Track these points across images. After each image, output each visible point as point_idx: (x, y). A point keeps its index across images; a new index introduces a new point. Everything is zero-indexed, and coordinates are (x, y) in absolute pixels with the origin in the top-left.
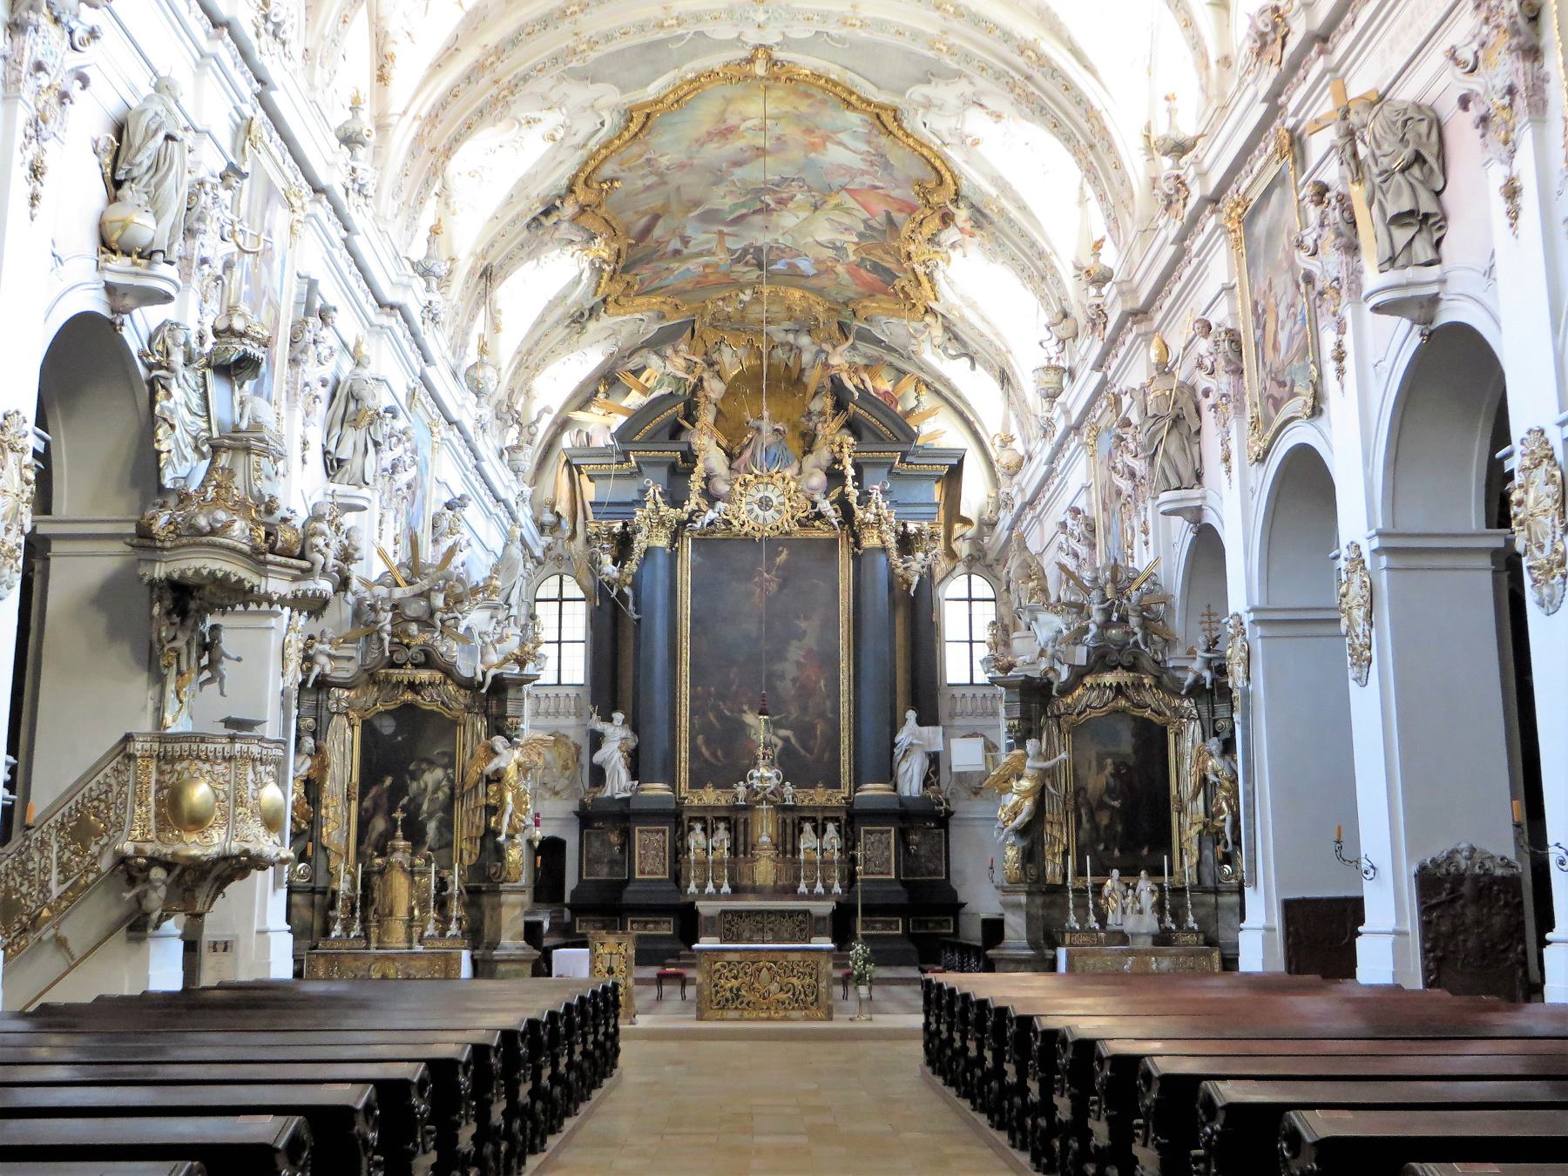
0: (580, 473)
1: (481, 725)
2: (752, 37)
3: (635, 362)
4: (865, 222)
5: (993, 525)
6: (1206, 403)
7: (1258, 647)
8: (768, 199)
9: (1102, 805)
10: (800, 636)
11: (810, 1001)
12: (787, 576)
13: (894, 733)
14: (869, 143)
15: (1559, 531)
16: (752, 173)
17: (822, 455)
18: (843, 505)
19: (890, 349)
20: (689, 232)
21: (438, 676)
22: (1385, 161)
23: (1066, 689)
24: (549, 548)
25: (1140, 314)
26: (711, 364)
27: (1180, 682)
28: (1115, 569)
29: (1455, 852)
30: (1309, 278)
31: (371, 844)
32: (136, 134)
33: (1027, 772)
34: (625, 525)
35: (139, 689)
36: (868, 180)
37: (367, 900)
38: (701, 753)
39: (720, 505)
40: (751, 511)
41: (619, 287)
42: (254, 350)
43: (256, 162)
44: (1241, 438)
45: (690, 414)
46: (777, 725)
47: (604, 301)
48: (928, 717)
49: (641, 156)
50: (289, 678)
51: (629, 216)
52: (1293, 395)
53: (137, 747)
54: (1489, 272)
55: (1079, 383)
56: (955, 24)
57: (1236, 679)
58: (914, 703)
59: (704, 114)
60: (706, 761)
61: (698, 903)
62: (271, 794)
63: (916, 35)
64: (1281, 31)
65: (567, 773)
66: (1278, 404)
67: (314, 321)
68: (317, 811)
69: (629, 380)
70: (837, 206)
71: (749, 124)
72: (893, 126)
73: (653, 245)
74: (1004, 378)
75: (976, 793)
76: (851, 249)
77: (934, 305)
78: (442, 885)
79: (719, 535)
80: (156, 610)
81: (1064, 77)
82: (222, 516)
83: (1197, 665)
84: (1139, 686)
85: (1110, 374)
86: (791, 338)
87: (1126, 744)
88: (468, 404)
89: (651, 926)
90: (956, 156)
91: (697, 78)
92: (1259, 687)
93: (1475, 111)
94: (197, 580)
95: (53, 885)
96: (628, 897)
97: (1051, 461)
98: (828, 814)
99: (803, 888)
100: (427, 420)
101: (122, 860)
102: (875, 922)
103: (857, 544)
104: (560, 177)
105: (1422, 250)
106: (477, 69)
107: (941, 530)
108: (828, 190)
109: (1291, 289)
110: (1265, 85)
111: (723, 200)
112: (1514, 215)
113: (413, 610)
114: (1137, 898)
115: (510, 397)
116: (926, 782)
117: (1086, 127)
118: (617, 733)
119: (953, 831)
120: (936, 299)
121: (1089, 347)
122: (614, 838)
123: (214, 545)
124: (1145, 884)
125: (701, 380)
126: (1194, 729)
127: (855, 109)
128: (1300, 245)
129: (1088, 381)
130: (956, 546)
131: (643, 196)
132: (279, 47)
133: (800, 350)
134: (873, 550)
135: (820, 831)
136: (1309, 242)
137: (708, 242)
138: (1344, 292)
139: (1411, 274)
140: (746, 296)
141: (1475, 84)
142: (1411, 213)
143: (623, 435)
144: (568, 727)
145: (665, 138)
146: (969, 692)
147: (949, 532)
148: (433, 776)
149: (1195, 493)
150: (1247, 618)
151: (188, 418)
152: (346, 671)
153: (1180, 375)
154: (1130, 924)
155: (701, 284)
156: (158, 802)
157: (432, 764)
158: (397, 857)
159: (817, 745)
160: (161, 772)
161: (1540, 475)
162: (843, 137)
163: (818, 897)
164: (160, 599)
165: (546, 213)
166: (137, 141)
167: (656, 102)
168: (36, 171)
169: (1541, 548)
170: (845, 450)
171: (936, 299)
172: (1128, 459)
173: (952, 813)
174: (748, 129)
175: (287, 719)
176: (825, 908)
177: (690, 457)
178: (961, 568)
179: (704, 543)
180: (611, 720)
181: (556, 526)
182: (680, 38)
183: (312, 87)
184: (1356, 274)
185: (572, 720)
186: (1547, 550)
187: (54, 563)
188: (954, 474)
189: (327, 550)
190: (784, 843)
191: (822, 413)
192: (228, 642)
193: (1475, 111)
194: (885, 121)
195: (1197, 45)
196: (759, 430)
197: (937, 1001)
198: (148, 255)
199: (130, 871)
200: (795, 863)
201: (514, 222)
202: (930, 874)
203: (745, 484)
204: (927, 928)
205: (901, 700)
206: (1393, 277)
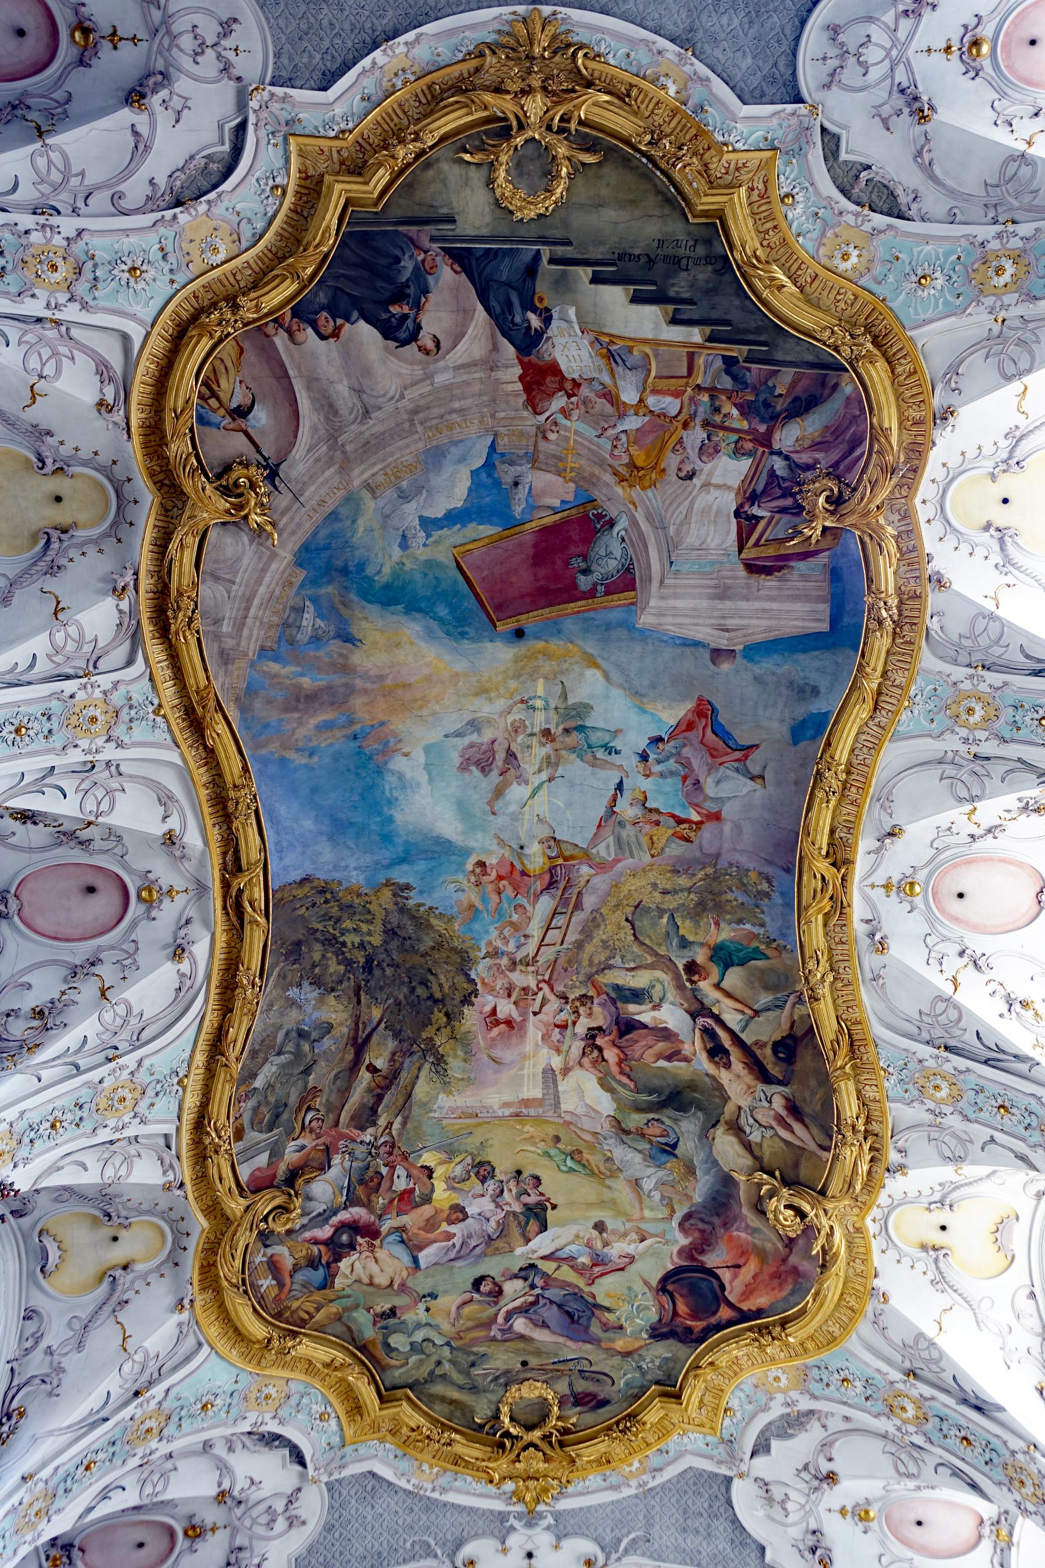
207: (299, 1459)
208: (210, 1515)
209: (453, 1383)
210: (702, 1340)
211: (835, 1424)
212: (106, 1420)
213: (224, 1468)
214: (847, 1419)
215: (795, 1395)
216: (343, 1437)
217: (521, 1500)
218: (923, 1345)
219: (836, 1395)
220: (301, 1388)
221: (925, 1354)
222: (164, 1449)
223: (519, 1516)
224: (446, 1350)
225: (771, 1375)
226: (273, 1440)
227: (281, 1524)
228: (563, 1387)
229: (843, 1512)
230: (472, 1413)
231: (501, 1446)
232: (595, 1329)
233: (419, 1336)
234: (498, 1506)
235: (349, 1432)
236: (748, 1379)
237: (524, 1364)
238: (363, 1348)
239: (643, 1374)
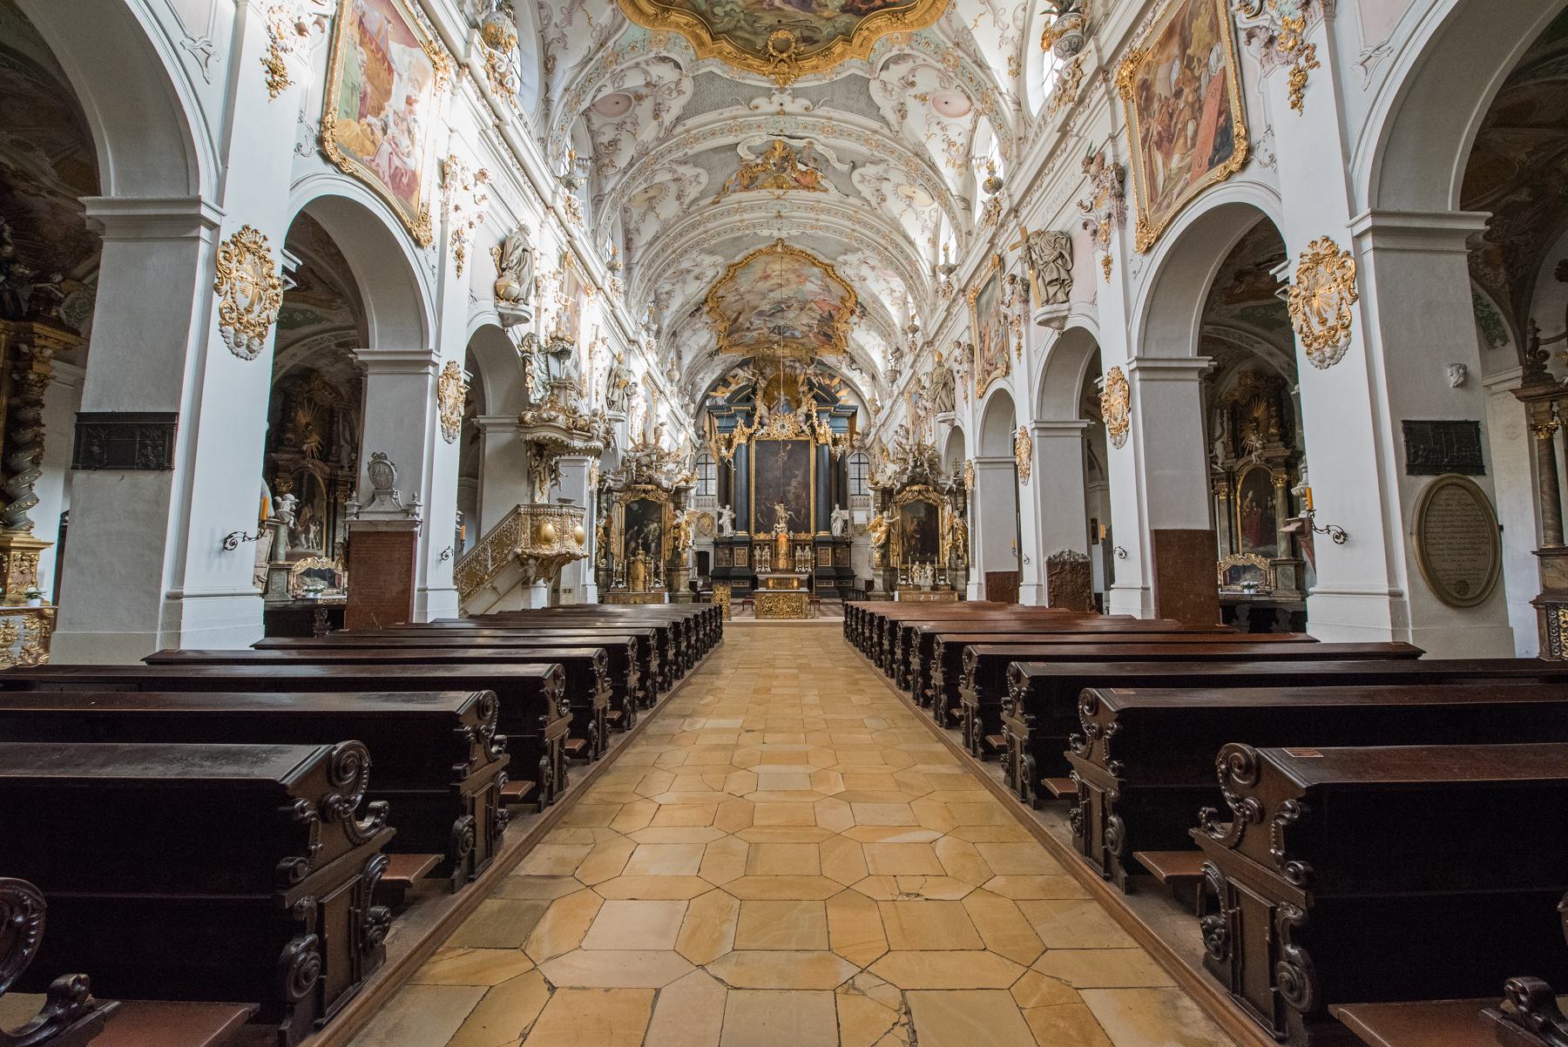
1: (672, 506)
2: (776, 234)
3: (733, 372)
6: (957, 376)
7: (978, 473)
8: (783, 306)
9: (913, 537)
10: (796, 476)
11: (797, 612)
12: (791, 454)
13: (831, 512)
15: (1126, 411)
16: (777, 295)
17: (804, 409)
18: (812, 426)
19: (830, 368)
20: (752, 320)
21: (655, 487)
22: (1046, 258)
23: (899, 492)
24: (701, 445)
25: (930, 343)
26: (762, 374)
27: (944, 489)
28: (919, 445)
29: (1063, 552)
30: (1006, 317)
31: (630, 552)
32: (509, 249)
33: (884, 524)
35: (523, 487)
36: (822, 297)
37: (628, 574)
41: (726, 343)
42: (567, 346)
43: (570, 273)
44: (972, 387)
45: (754, 392)
48: (844, 507)
50: (593, 486)
51: (729, 313)
52: (996, 368)
53: (522, 510)
54: (1093, 303)
55: (903, 376)
56: (857, 227)
57: (969, 486)
58: (838, 502)
59: (758, 269)
62: (580, 529)
63: (841, 233)
64: (998, 209)
66: (989, 373)
67: (599, 343)
68: (609, 540)
69: (731, 380)
70: (810, 309)
72: (831, 273)
74: (874, 377)
75: (861, 535)
78: (657, 567)
80: (529, 454)
81: (901, 248)
82: (553, 413)
83: (950, 482)
84: (927, 491)
87: (922, 514)
90: (856, 285)
92: (978, 489)
93: (1090, 228)
94: (545, 442)
95: (489, 566)
96: (732, 574)
97: (891, 408)
99: (797, 570)
101: (517, 556)
104: (702, 296)
105: (1061, 296)
106: (667, 245)
107: (848, 437)
108: (807, 302)
109: (997, 324)
110: (989, 235)
112: (1108, 274)
113: (645, 460)
114: (925, 573)
116: (843, 531)
117: (909, 268)
118: (727, 513)
121: (909, 359)
123: (550, 426)
124: (928, 567)
126: (949, 508)
127: (817, 266)
128: (1003, 303)
129: (907, 373)
132: (576, 220)
133: (796, 368)
134: (823, 445)
135: (803, 549)
136: (1007, 301)
138: (1022, 320)
139: (1055, 306)
140: (775, 346)
141: (1091, 216)
142: (1057, 280)
143: (729, 400)
145: (743, 279)
146: (859, 497)
147: (851, 437)
148: (654, 526)
149: (952, 413)
150: (973, 462)
151: (541, 375)
152: (619, 485)
153: (947, 366)
154: (922, 583)
155: (758, 342)
156: (531, 532)
157: (653, 521)
158: (640, 557)
159: (802, 517)
160: (532, 520)
161: (1118, 387)
162: (812, 279)
163: (803, 573)
164: (530, 449)
165: (696, 310)
166: (510, 250)
168: (459, 256)
169: (1116, 420)
172: (924, 402)
175: (592, 502)
176: (805, 577)
177: (754, 409)
178: (856, 451)
179: (758, 442)
181: (704, 437)
182: (748, 235)
183: (596, 246)
184: (1027, 313)
185: (711, 508)
186: (1119, 421)
187: (487, 435)
188: (854, 414)
189: (599, 427)
192: (562, 469)
193: (1090, 228)
194: (829, 270)
195: (957, 228)
197: (849, 612)
198: (517, 300)
199: (521, 560)
201: (684, 313)
203: (775, 420)
205: (833, 501)
206: (1047, 308)
207: (678, 66)
208: (644, 91)
209: (745, 30)
210: (865, 15)
211: (919, 62)
212: (592, 59)
213: (646, 73)
214: (924, 60)
215: (903, 46)
216: (697, 57)
217: (778, 83)
218: (966, 32)
219: (922, 49)
220: (675, 35)
221: (965, 37)
222: (619, 68)
223: (776, 89)
224: (742, 15)
225: (895, 35)
226: (664, 60)
227: (674, 94)
228: (797, 33)
229: (916, 97)
230: (755, 44)
231: (769, 60)
232: (814, 6)
233: (728, 8)
234: (768, 85)
235: (699, 54)
236: (884, 34)
237: (779, 21)
238: (702, 14)
239: (836, 29)
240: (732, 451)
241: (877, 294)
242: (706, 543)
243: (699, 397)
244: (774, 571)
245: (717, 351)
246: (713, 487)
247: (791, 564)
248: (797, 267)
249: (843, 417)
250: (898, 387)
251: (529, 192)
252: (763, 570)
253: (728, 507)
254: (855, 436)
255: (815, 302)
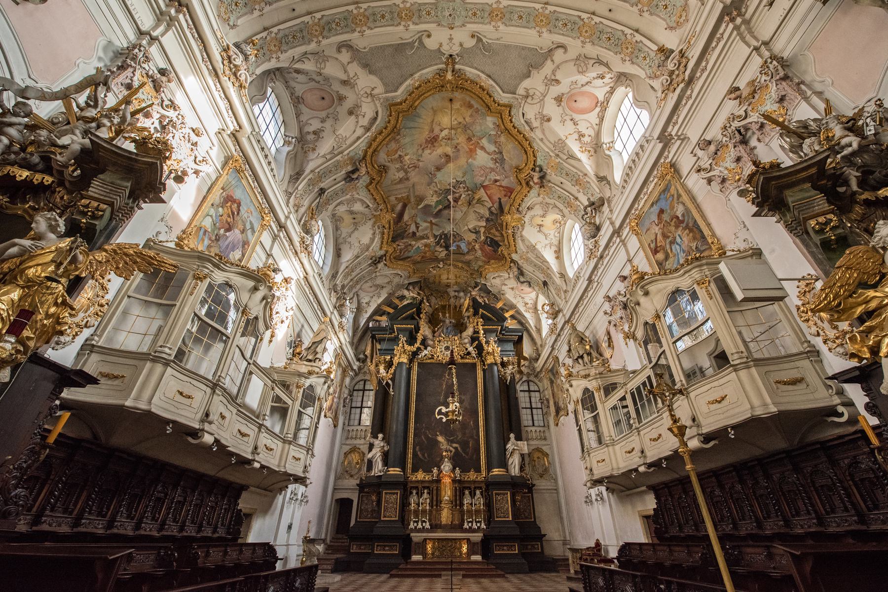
0: (376, 341)
4: (489, 209)
5: (538, 360)
8: (450, 198)
13: (505, 446)
14: (496, 142)
17: (470, 331)
20: (418, 220)
24: (360, 368)
34: (391, 358)
36: (493, 176)
38: (418, 455)
39: (429, 348)
40: (441, 352)
45: (419, 312)
46: (452, 442)
47: (385, 255)
48: (519, 438)
49: (396, 151)
58: (511, 431)
60: (420, 459)
61: (412, 534)
65: (358, 466)
71: (443, 134)
73: (405, 226)
75: (541, 476)
76: (482, 230)
77: (515, 257)
79: (429, 361)
85: (673, 133)
86: (456, 294)
88: (291, 216)
89: (387, 548)
91: (420, 86)
97: (590, 280)
98: (477, 485)
99: (466, 526)
100: (257, 205)
102: (504, 546)
103: (484, 365)
111: (432, 200)
115: (343, 287)
116: (522, 468)
118: (379, 443)
119: (535, 496)
120: (516, 252)
122: (374, 498)
125: (423, 299)
130: (523, 369)
131: (399, 186)
134: (491, 365)
135: (472, 495)
137: (426, 229)
144: (361, 444)
145: (407, 140)
146: (533, 429)
159: (470, 451)
162: (484, 142)
163: (474, 531)
165: (353, 172)
167: (401, 103)
170: (479, 324)
171: (516, 252)
173: (534, 485)
174: (443, 138)
176: (477, 537)
177: (417, 329)
180: (377, 438)
181: (364, 361)
185: (362, 441)
188: (520, 339)
190: (456, 502)
191: (468, 317)
196: (444, 322)
200: (462, 513)
201: (337, 166)
202: (526, 518)
203: (439, 341)
204: (527, 549)
240: (392, 370)
241: (564, 138)
242: (350, 488)
243: (362, 322)
244: (435, 527)
245: (381, 258)
246: (367, 418)
247: (457, 516)
248: (468, 119)
249: (509, 341)
250: (612, 223)
251: (286, 244)
252: (420, 526)
253: (380, 436)
254: (523, 362)
255: (485, 187)
